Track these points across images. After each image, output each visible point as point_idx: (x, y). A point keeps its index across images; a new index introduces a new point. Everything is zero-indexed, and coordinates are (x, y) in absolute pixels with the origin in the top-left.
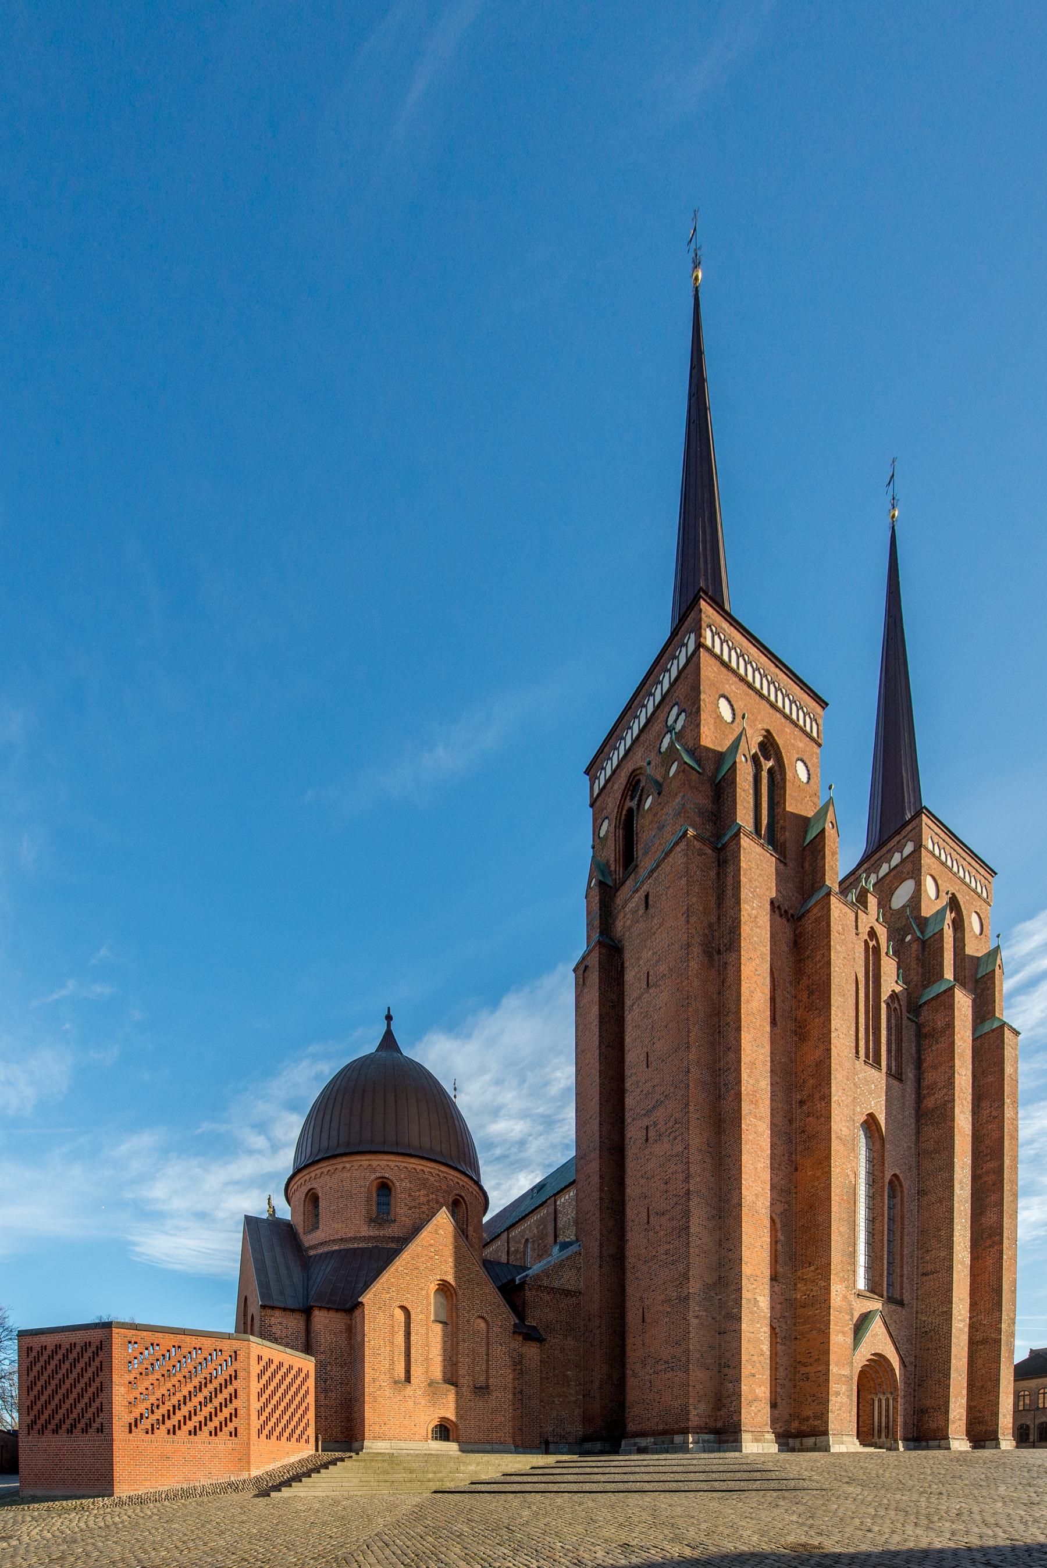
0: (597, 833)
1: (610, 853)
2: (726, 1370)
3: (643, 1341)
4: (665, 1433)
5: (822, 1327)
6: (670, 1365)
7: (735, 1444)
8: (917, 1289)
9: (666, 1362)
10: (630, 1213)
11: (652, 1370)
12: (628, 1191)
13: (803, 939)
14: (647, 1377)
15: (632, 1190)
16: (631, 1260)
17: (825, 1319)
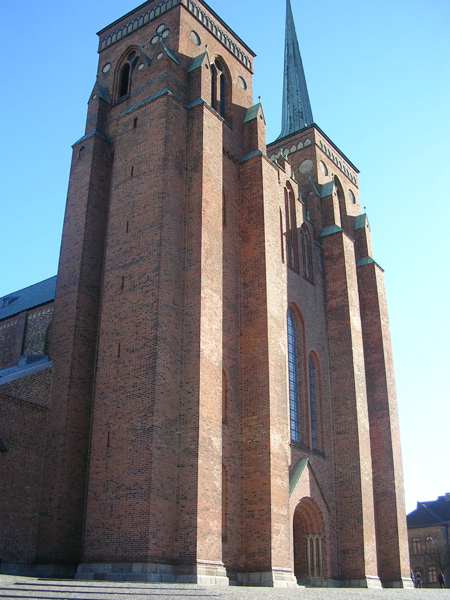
0: (101, 69)
1: (111, 83)
2: (183, 502)
3: (106, 464)
4: (124, 560)
5: (264, 469)
6: (132, 492)
7: (190, 576)
8: (334, 445)
9: (129, 488)
10: (103, 343)
11: (114, 495)
12: (103, 325)
13: (244, 176)
14: (109, 501)
15: (105, 325)
16: (100, 386)
17: (266, 463)
